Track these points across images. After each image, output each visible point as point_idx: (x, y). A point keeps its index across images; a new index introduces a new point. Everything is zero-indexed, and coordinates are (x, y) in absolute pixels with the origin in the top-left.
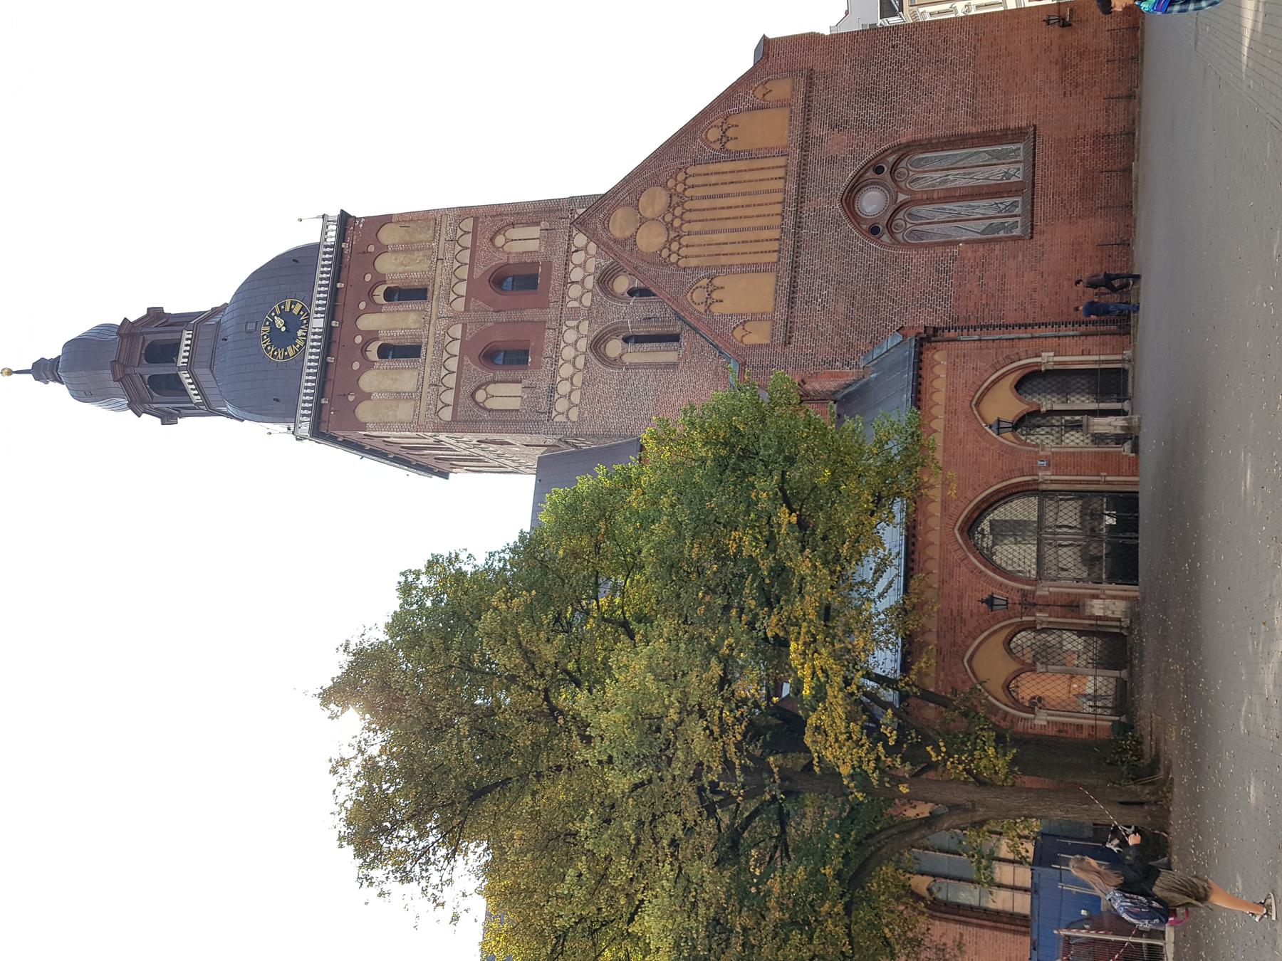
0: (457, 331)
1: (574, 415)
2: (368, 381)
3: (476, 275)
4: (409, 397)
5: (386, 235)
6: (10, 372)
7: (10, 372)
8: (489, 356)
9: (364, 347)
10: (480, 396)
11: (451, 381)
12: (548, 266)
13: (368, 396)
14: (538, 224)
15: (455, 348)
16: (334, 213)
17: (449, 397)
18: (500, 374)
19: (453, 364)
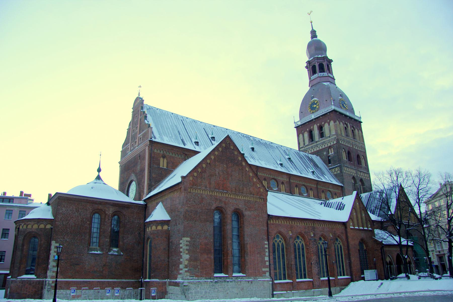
0: (351, 146)
1: (345, 172)
2: (341, 123)
3: (359, 152)
4: (341, 134)
5: (360, 132)
6: (311, 23)
7: (311, 23)
8: (349, 153)
9: (346, 124)
10: (343, 150)
11: (345, 144)
12: (361, 167)
13: (340, 124)
14: (366, 165)
15: (349, 145)
16: (362, 120)
17: (343, 143)
18: (347, 154)
19: (347, 145)
